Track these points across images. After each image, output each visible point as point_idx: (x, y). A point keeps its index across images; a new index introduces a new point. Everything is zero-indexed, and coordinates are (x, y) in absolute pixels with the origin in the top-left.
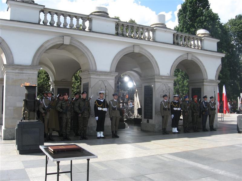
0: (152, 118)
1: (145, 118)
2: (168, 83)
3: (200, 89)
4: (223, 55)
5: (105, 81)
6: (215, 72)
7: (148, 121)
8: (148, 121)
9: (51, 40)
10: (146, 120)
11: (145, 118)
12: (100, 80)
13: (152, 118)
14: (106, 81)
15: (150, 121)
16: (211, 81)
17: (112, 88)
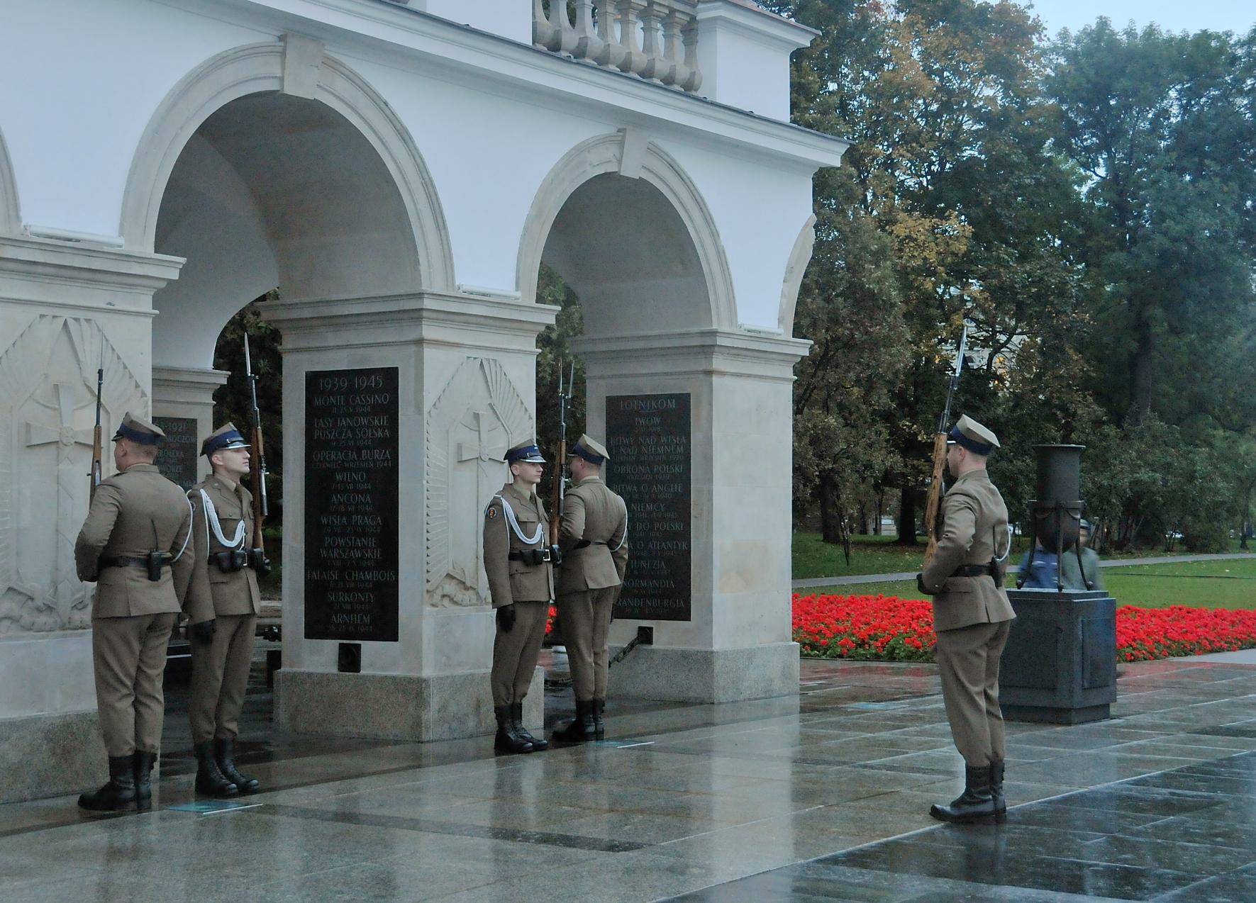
0: (387, 629)
1: (313, 631)
2: (503, 359)
3: (683, 401)
4: (830, 155)
5: (77, 320)
6: (779, 286)
7: (350, 660)
8: (350, 660)
11: (313, 631)
12: (42, 316)
13: (387, 629)
14: (88, 320)
15: (370, 650)
16: (755, 350)
17: (137, 386)
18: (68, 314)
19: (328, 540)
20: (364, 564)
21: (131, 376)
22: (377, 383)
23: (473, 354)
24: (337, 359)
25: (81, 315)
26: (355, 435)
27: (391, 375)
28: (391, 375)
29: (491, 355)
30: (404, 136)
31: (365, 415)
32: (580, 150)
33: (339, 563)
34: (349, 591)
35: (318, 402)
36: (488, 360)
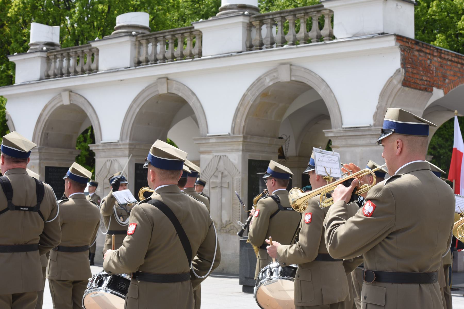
2: (227, 154)
9: (50, 103)
18: (112, 159)
25: (114, 159)
29: (224, 154)
30: (194, 94)
32: (259, 79)
36: (223, 156)
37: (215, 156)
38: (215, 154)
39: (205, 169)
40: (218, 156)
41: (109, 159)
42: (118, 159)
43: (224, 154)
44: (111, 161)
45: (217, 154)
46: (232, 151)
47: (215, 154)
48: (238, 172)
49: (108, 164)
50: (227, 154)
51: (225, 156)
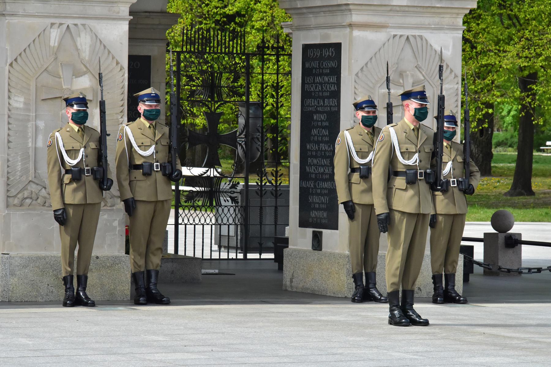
1: (303, 224)
2: (426, 34)
10: (309, 231)
11: (303, 224)
12: (52, 24)
14: (84, 25)
15: (326, 233)
17: (117, 63)
18: (70, 22)
19: (310, 160)
20: (324, 177)
21: (113, 58)
22: (332, 53)
23: (399, 32)
24: (315, 38)
26: (322, 88)
27: (338, 47)
28: (338, 47)
29: (417, 33)
31: (327, 75)
33: (313, 176)
34: (318, 195)
35: (307, 65)
36: (414, 36)
37: (395, 36)
38: (394, 32)
39: (366, 64)
40: (401, 36)
41: (57, 21)
42: (92, 23)
43: (417, 33)
44: (65, 27)
45: (399, 32)
46: (439, 28)
47: (394, 32)
48: (453, 75)
49: (54, 36)
50: (426, 34)
51: (421, 37)
